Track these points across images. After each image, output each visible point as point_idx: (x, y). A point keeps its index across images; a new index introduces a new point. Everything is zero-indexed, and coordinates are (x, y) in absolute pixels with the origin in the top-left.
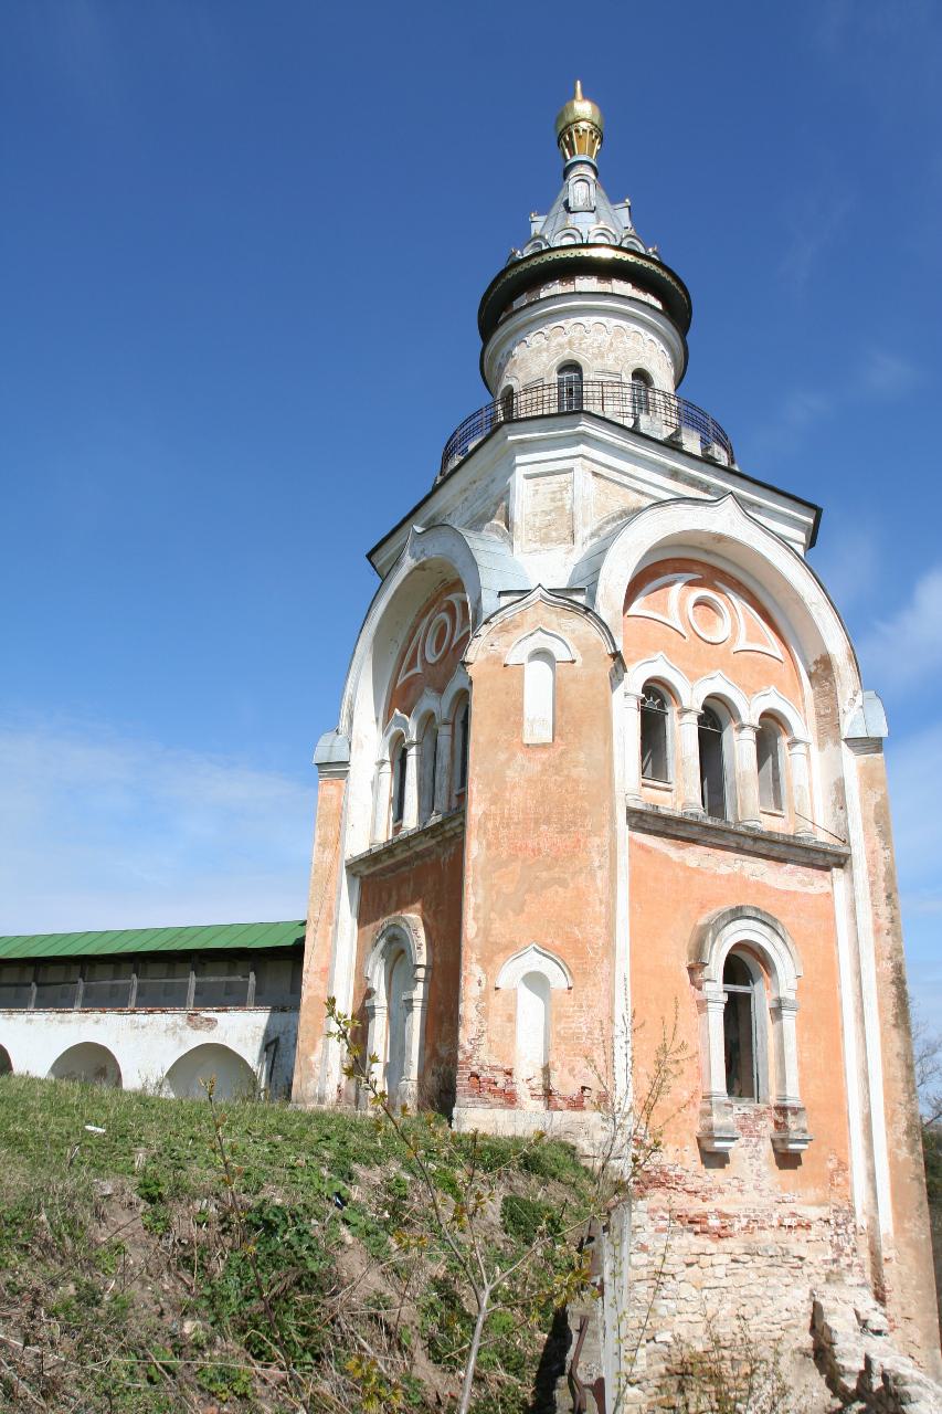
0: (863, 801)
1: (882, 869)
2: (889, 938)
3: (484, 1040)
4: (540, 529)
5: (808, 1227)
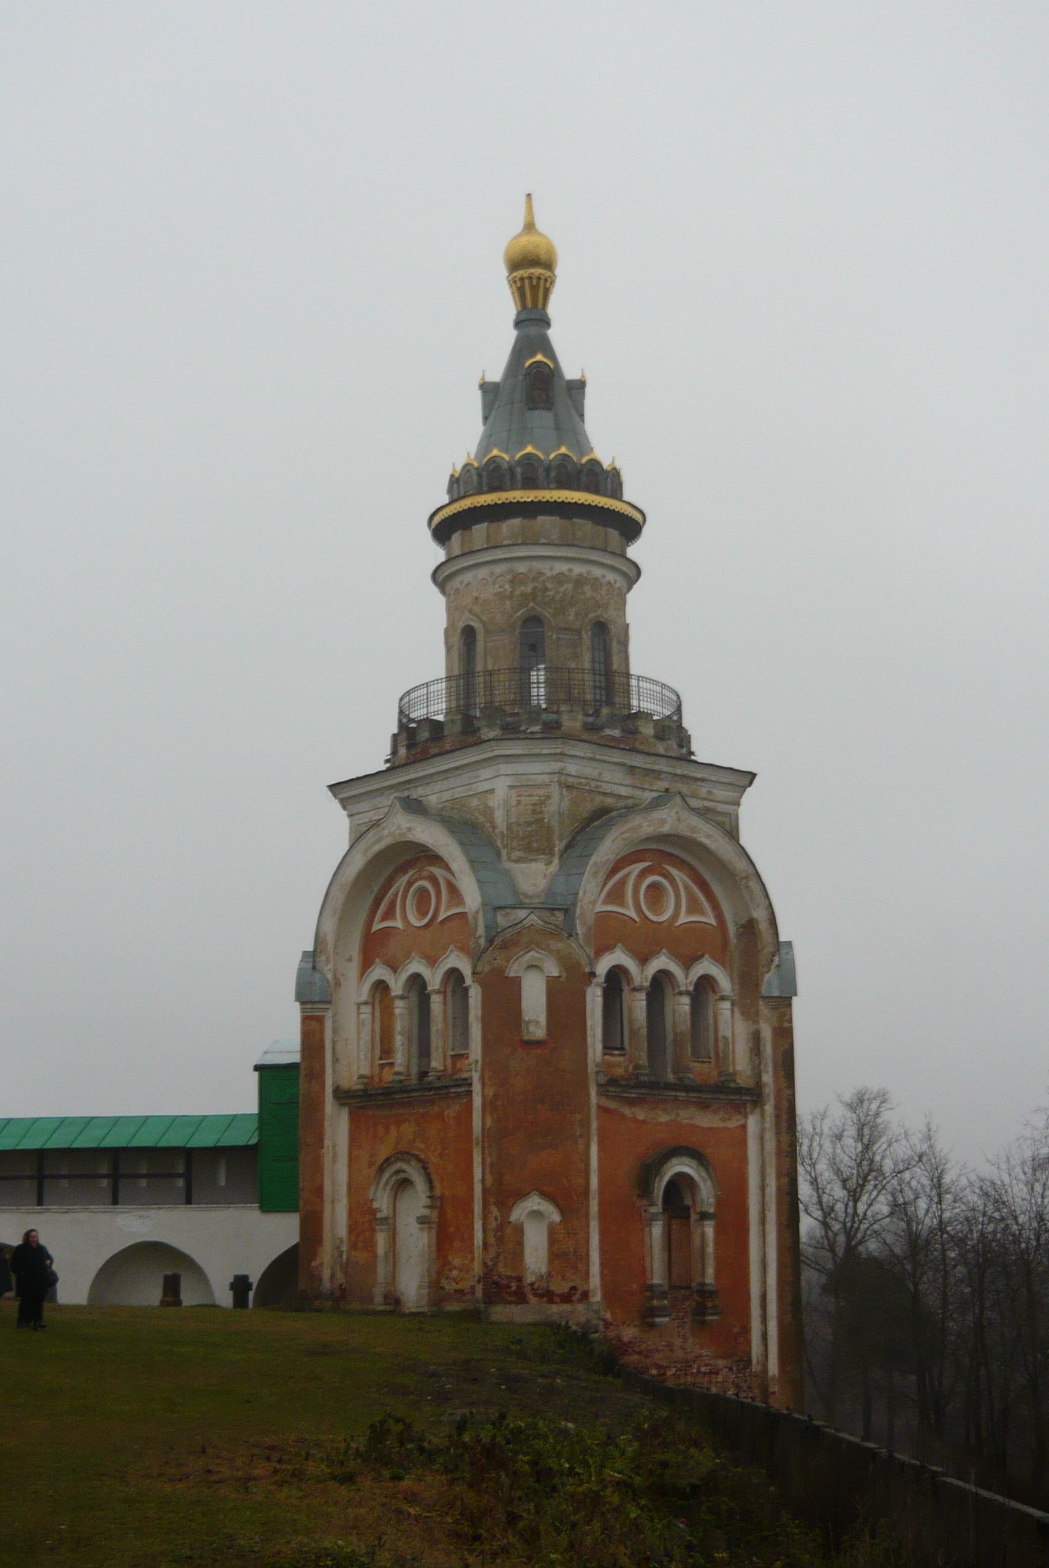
0: (775, 1048)
1: (786, 1104)
2: (788, 1159)
3: (501, 1257)
4: (523, 839)
5: (717, 1373)
